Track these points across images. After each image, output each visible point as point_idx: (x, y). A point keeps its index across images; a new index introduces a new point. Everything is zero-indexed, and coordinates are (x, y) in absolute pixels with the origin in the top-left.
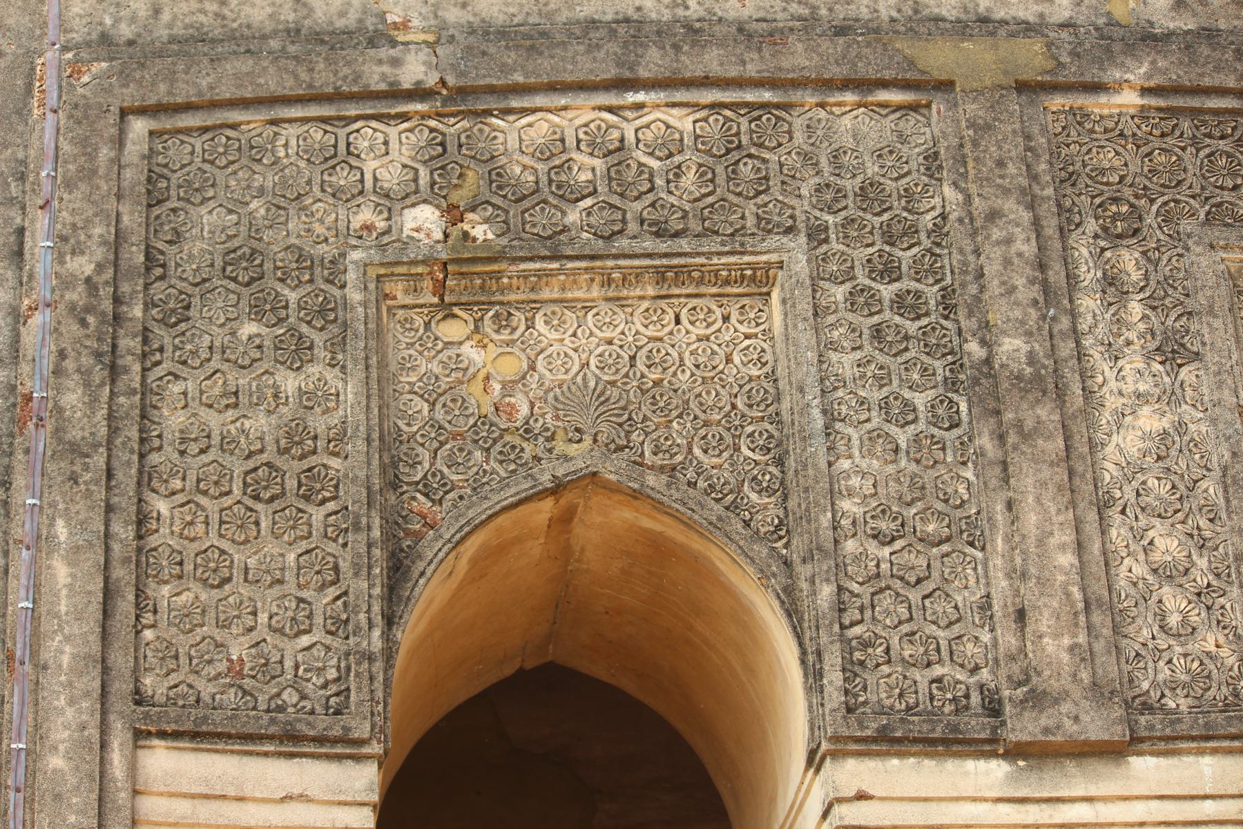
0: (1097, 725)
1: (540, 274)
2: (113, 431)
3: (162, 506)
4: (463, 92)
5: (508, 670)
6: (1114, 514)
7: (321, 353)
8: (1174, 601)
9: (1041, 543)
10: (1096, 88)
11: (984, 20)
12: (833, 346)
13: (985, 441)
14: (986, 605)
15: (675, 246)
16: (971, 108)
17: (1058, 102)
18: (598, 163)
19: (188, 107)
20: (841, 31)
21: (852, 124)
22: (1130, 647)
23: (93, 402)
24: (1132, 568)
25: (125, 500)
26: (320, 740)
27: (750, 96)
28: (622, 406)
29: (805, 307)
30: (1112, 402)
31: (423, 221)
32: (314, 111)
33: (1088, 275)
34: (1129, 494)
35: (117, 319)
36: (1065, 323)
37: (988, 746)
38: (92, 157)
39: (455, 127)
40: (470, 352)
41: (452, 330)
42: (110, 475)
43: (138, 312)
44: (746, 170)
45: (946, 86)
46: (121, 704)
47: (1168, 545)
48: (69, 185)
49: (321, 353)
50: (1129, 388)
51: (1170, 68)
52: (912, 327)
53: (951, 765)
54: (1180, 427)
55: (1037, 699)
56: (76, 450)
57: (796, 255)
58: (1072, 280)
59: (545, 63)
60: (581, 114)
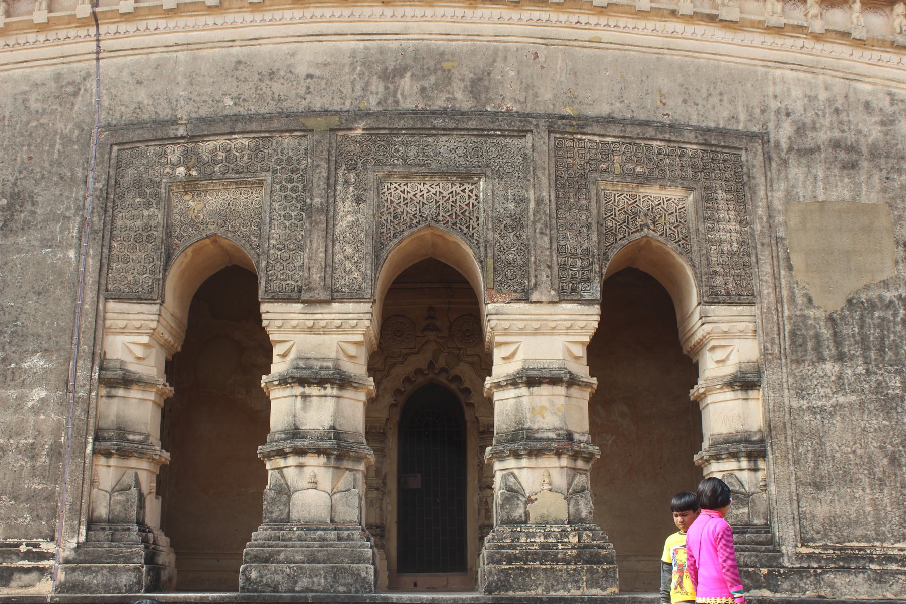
0: (323, 296)
1: (208, 184)
2: (104, 226)
3: (115, 244)
4: (193, 137)
5: (224, 267)
6: (337, 243)
7: (154, 206)
8: (349, 265)
9: (316, 251)
10: (351, 129)
11: (326, 111)
12: (275, 201)
13: (307, 225)
14: (302, 266)
15: (239, 174)
16: (317, 137)
17: (340, 133)
18: (224, 154)
19: (127, 143)
20: (288, 116)
21: (288, 141)
22: (335, 276)
23: (100, 220)
24: (339, 257)
25: (106, 243)
26: (146, 300)
27: (262, 135)
28: (224, 216)
29: (269, 191)
30: (341, 214)
31: (181, 170)
32: (157, 143)
33: (341, 180)
34: (342, 237)
35: (107, 198)
36: (332, 193)
37: (298, 301)
38: (103, 157)
39: (191, 146)
40: (191, 203)
41: (187, 198)
42: (103, 237)
43: (112, 196)
44: (260, 155)
45: (311, 130)
46: (102, 292)
47: (349, 250)
48: (97, 165)
49: (154, 206)
50: (346, 210)
51: (370, 122)
52: (294, 195)
53: (289, 305)
54: (357, 220)
55: (310, 290)
56: (95, 232)
57: (268, 177)
58: (336, 181)
59: (213, 128)
60: (221, 141)
